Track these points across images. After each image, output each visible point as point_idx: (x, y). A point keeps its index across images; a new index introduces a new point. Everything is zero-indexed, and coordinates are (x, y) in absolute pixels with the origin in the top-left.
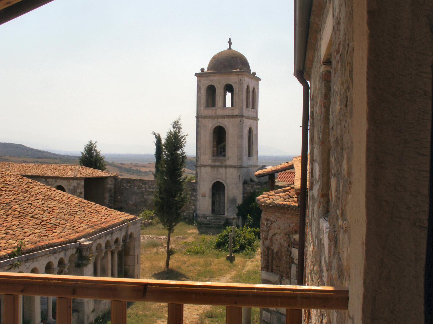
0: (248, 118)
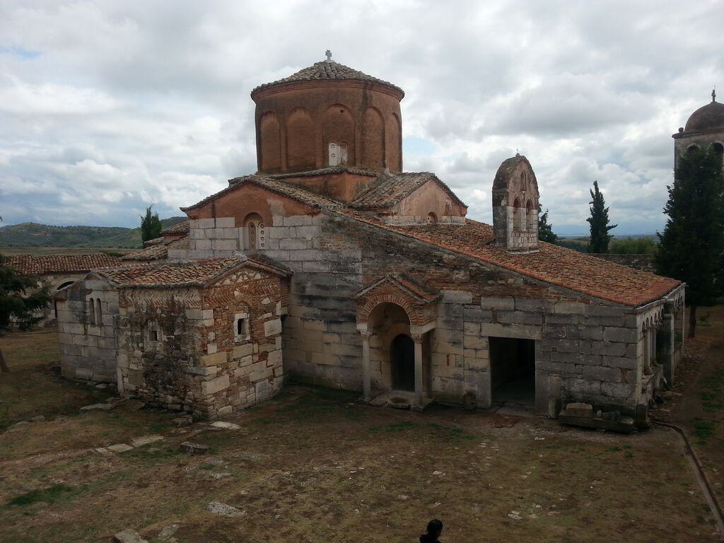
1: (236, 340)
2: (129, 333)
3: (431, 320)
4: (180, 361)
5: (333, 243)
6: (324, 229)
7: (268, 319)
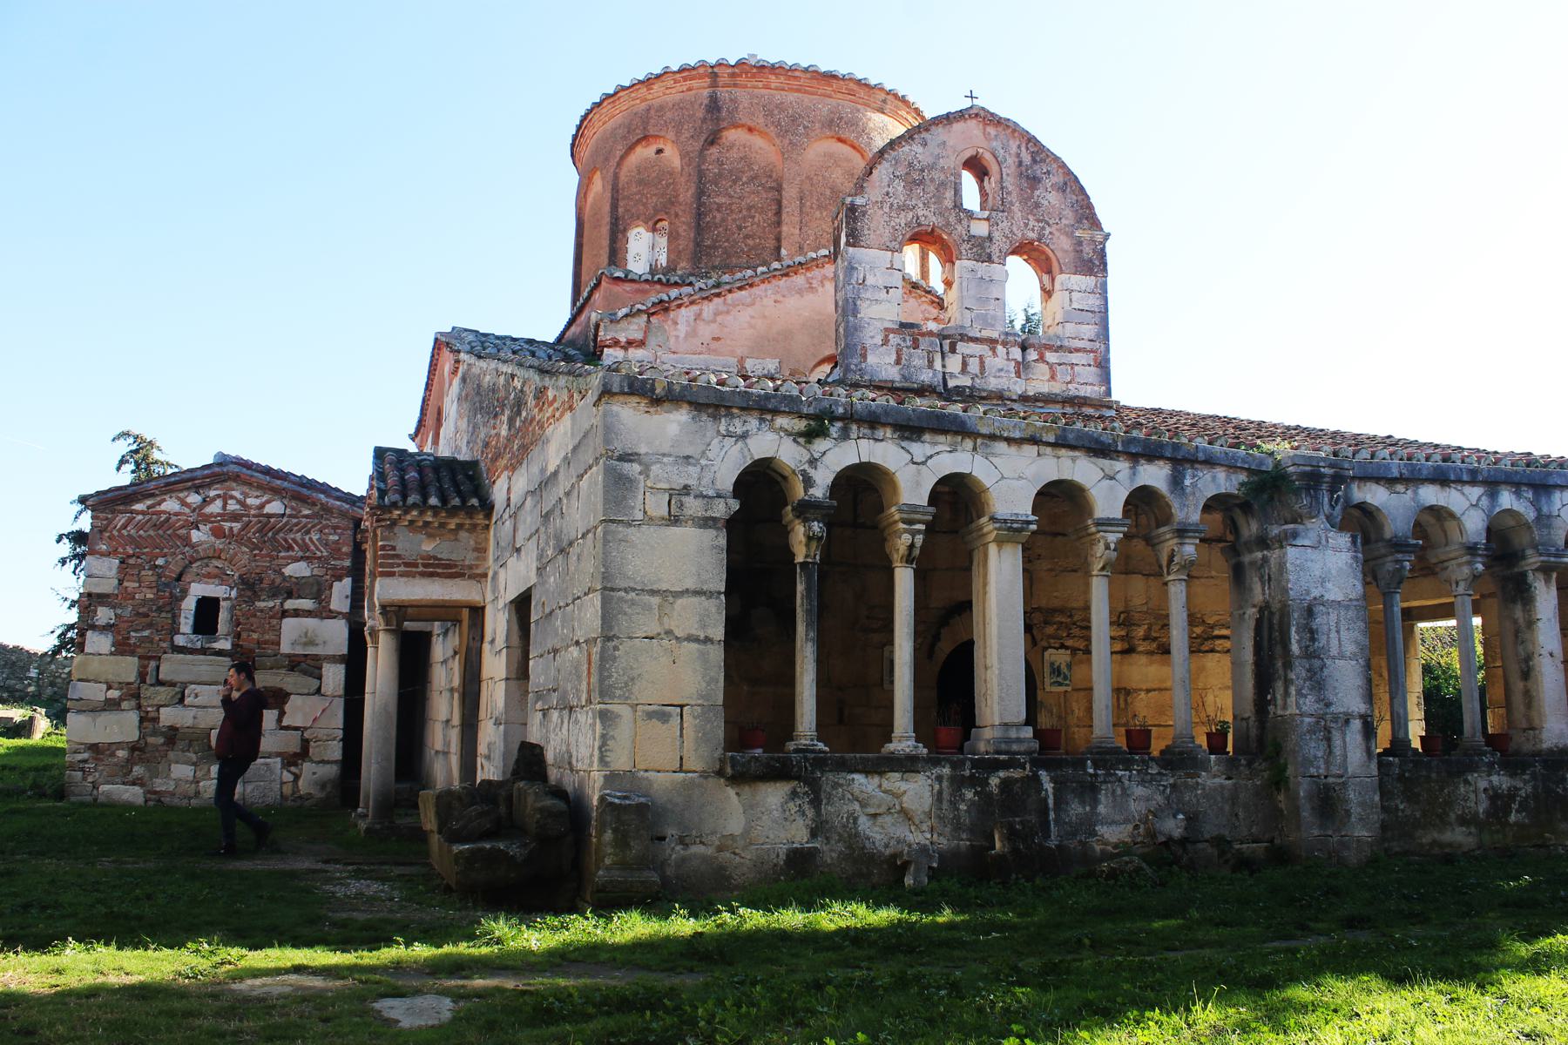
7: (297, 613)
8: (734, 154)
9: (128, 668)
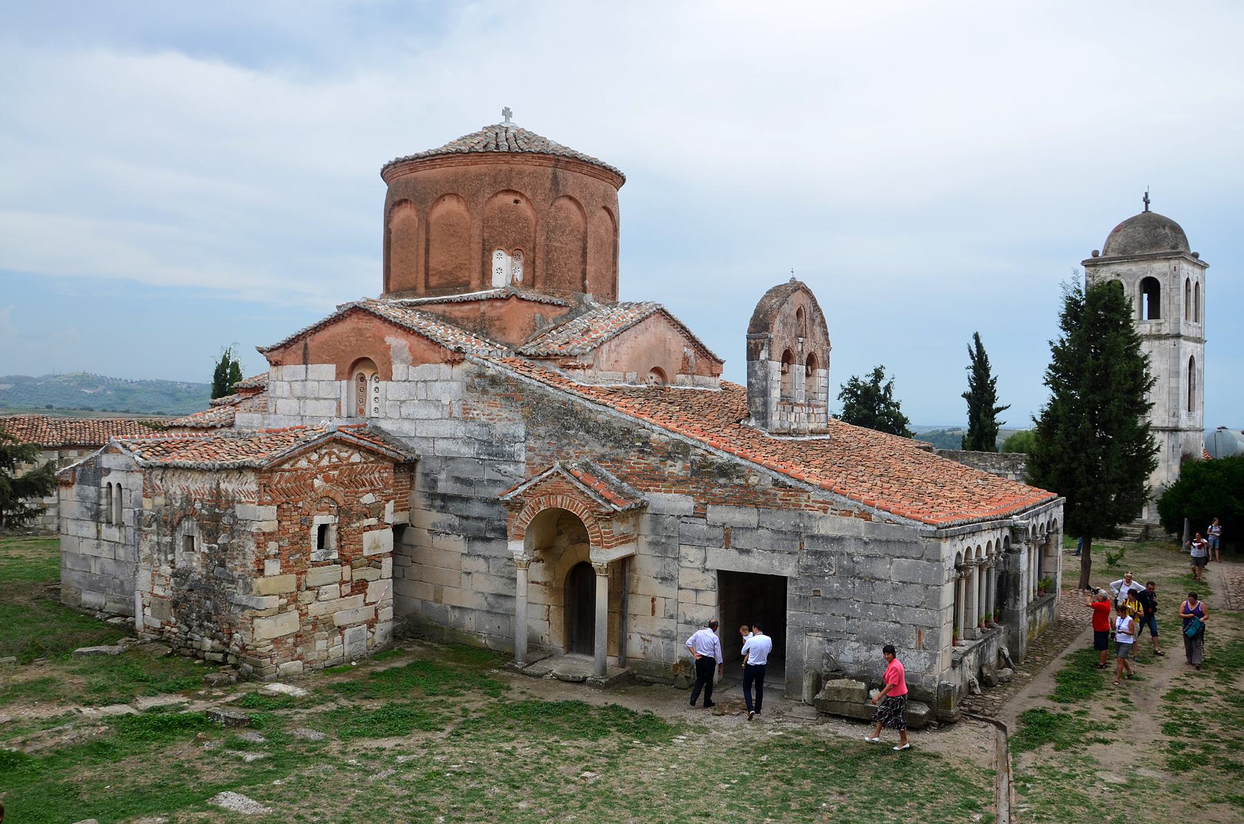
0: (1188, 339)
1: (313, 557)
2: (155, 538)
3: (625, 539)
4: (225, 584)
5: (481, 411)
6: (470, 388)
7: (370, 528)
8: (562, 214)
9: (290, 581)
